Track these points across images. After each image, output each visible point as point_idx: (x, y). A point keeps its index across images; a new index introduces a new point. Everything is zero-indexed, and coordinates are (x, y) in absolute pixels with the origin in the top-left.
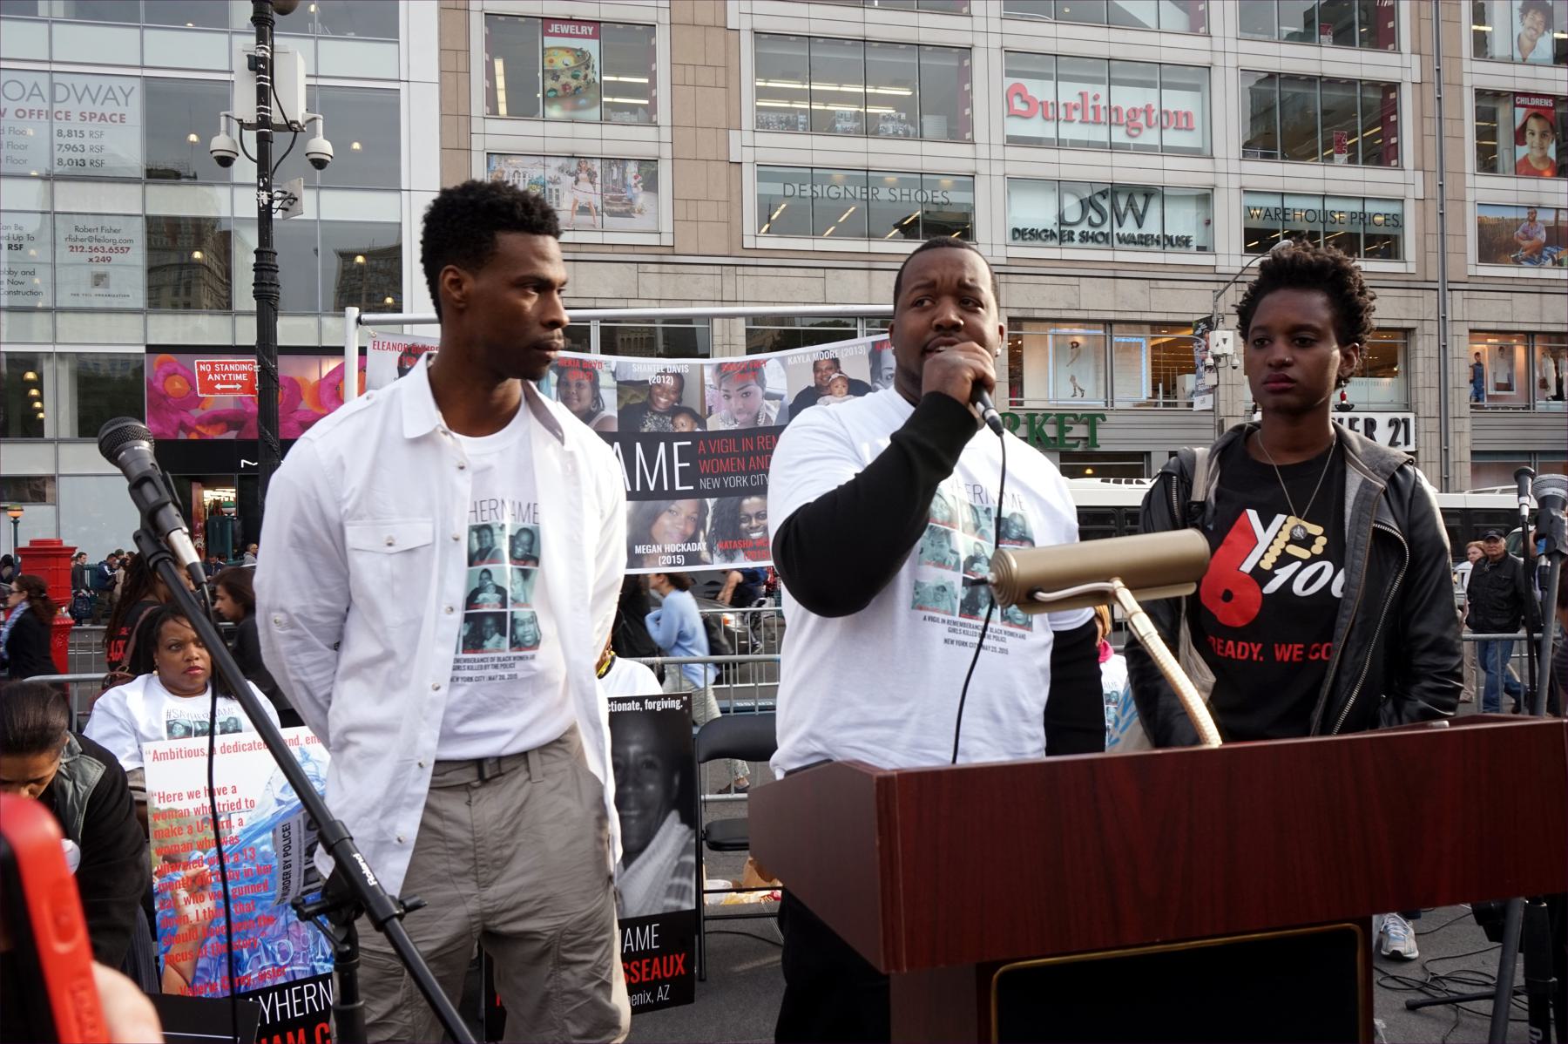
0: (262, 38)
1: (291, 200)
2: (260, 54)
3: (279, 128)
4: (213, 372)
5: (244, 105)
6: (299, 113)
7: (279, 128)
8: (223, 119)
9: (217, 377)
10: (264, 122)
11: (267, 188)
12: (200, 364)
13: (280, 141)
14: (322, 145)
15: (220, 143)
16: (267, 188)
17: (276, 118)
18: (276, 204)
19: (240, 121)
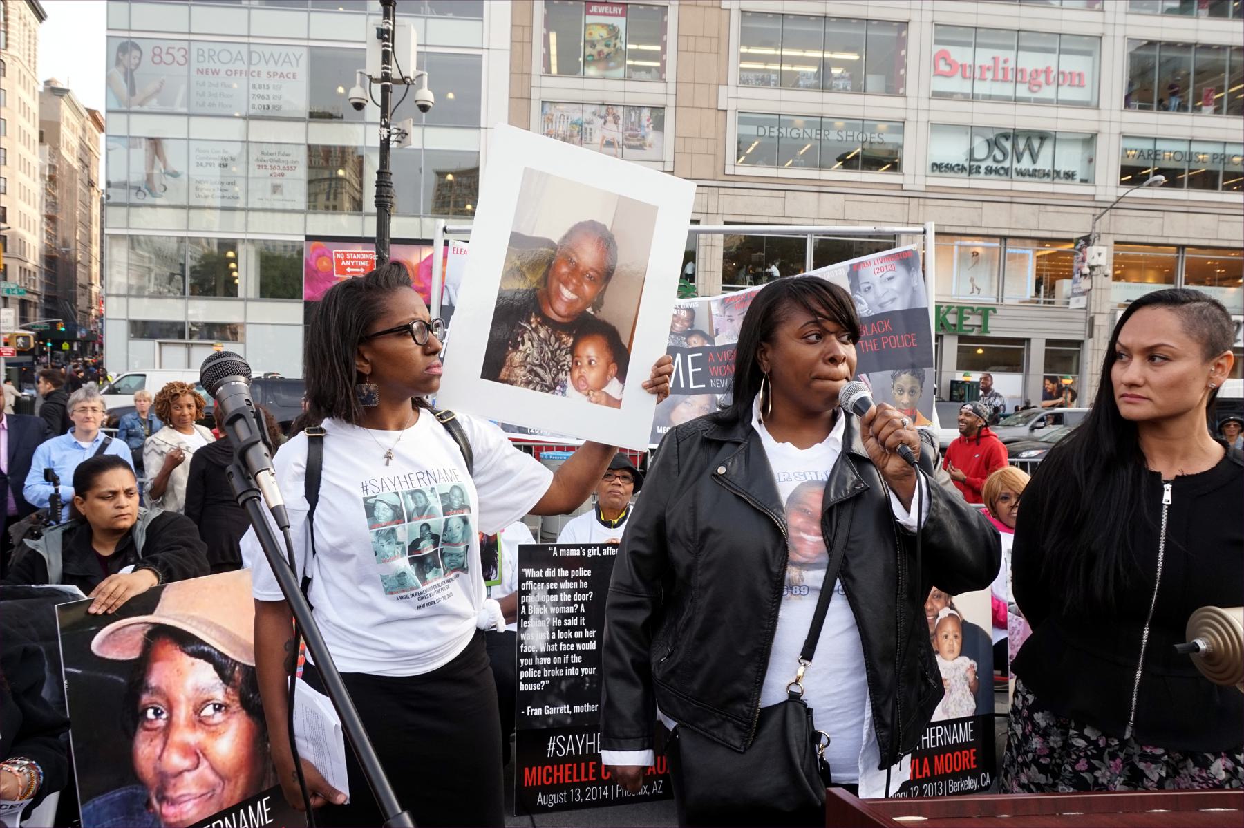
0: (386, 15)
1: (403, 134)
2: (385, 27)
3: (396, 82)
4: (345, 259)
5: (374, 67)
6: (411, 71)
7: (396, 82)
8: (358, 75)
9: (348, 263)
10: (386, 77)
11: (387, 126)
12: (338, 252)
13: (397, 91)
14: (426, 95)
15: (357, 93)
16: (387, 126)
17: (395, 75)
18: (393, 138)
19: (370, 77)
